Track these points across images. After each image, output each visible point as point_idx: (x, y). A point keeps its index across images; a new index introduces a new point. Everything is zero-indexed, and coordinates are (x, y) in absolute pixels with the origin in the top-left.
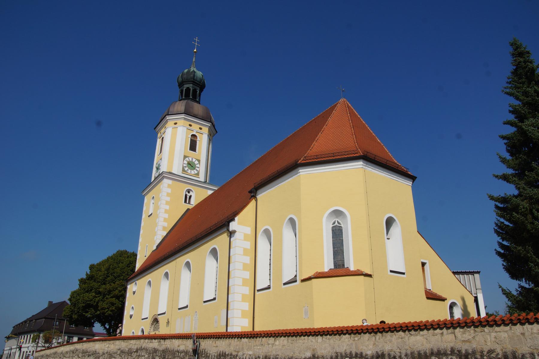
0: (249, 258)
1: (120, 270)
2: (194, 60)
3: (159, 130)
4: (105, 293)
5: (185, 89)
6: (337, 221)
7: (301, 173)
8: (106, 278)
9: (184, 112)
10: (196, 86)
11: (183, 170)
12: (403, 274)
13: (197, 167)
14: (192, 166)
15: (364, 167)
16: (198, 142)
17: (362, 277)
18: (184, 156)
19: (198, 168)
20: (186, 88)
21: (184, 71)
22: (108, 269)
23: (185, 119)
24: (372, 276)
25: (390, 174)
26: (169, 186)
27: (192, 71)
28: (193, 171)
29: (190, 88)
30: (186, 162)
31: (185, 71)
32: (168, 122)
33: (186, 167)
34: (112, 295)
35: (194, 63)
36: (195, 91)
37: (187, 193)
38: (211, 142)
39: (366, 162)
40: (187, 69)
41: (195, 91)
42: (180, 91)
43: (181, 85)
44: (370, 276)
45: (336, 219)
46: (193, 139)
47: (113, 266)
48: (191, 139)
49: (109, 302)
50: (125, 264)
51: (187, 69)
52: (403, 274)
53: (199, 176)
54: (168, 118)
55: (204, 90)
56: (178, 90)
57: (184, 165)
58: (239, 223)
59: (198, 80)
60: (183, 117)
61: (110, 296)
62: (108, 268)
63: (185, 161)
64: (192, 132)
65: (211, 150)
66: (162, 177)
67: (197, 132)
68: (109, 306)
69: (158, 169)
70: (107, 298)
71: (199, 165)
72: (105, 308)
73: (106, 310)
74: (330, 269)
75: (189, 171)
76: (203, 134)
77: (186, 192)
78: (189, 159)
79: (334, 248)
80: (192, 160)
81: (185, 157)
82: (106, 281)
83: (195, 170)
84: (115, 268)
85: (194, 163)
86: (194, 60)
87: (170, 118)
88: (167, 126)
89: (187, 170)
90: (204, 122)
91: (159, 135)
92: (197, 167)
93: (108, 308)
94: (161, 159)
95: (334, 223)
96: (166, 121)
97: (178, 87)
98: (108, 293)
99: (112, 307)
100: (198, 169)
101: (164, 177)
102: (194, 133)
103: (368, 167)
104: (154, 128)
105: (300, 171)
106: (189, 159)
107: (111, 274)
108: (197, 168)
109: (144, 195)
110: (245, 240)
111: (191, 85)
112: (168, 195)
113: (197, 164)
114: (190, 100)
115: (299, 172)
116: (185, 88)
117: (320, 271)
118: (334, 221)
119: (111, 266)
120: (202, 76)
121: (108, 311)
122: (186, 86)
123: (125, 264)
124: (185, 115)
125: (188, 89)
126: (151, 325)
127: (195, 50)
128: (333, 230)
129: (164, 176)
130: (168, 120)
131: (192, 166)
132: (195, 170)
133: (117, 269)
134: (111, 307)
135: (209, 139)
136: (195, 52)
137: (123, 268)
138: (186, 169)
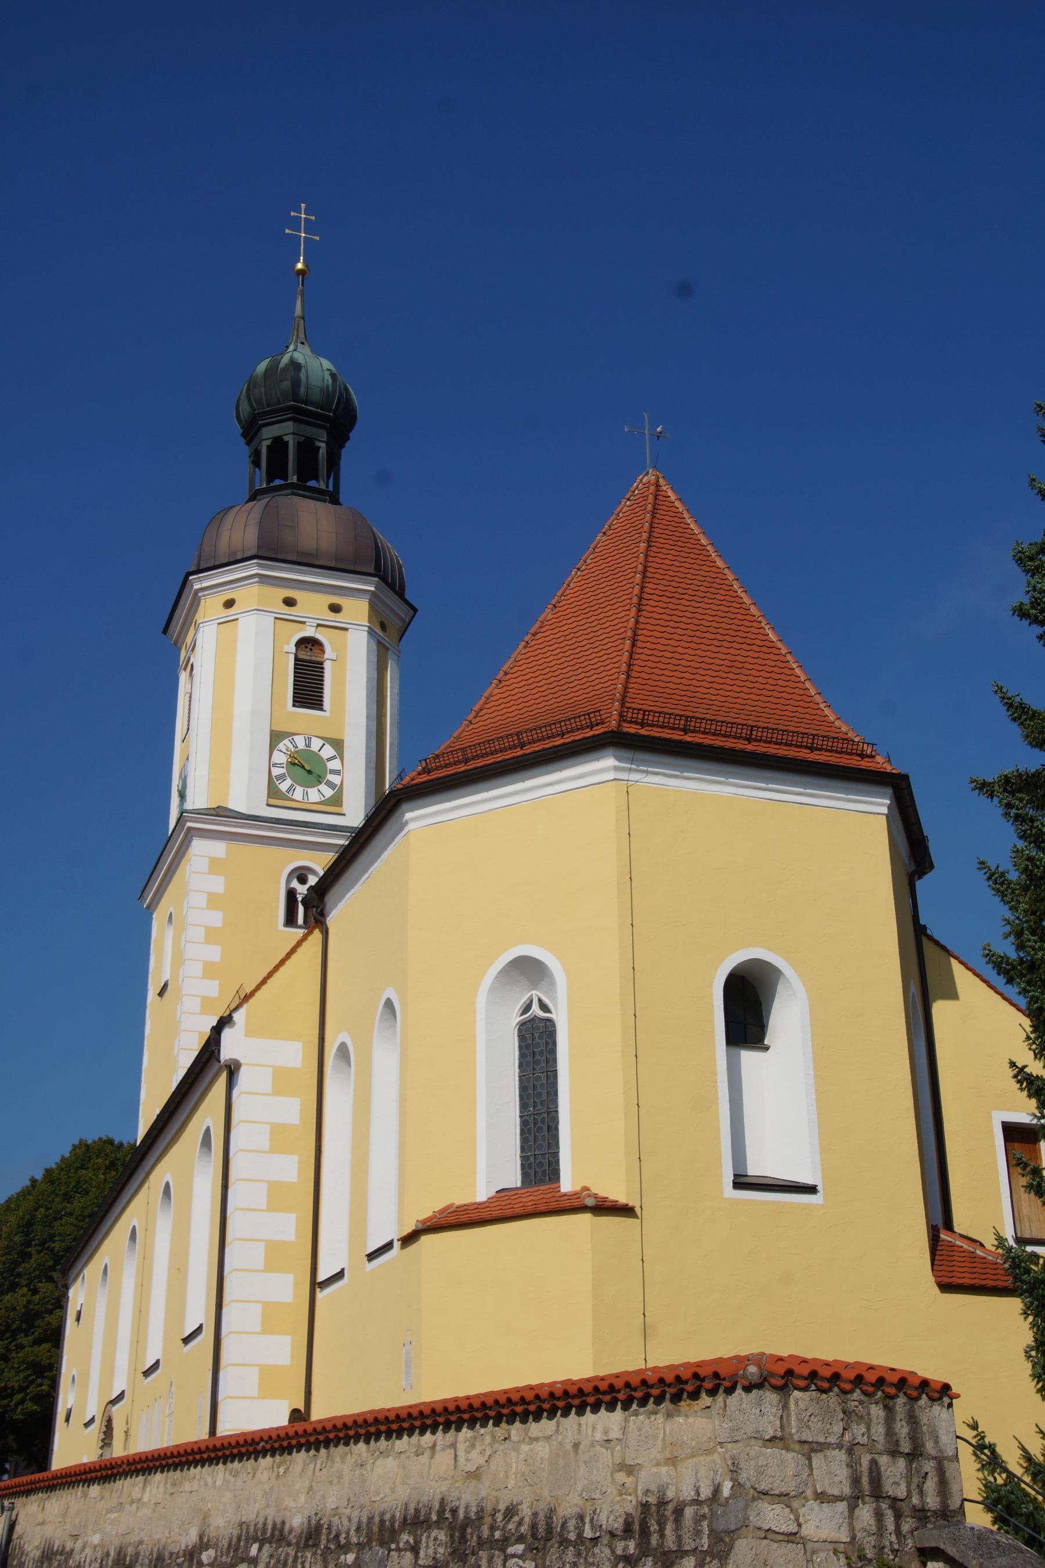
0: (295, 1159)
1: (75, 1226)
2: (298, 310)
4: (14, 1326)
6: (540, 1000)
7: (411, 826)
8: (17, 1264)
9: (254, 552)
10: (309, 428)
11: (273, 792)
12: (811, 1190)
13: (333, 772)
14: (309, 772)
15: (624, 776)
16: (328, 666)
17: (586, 1218)
18: (272, 732)
19: (337, 772)
20: (268, 442)
21: (253, 372)
22: (27, 1226)
23: (263, 579)
24: (638, 1210)
25: (763, 785)
26: (215, 866)
27: (286, 366)
28: (316, 788)
29: (286, 438)
30: (280, 758)
31: (259, 367)
32: (202, 602)
33: (282, 777)
34: (38, 1332)
35: (302, 322)
36: (307, 448)
37: (295, 884)
38: (390, 654)
39: (628, 754)
40: (268, 360)
41: (307, 448)
42: (252, 458)
43: (250, 430)
44: (626, 1211)
45: (534, 992)
46: (303, 655)
47: (47, 1209)
48: (296, 659)
49: (23, 1362)
50: (96, 1198)
51: (268, 360)
52: (811, 1190)
53: (341, 806)
54: (197, 586)
55: (351, 435)
56: (244, 451)
57: (276, 772)
58: (251, 1032)
59: (316, 396)
60: (255, 571)
61: (30, 1338)
62: (28, 1221)
63: (276, 753)
64: (301, 630)
65: (396, 691)
66: (186, 836)
67: (319, 625)
68: (26, 1378)
69: (182, 796)
70: (22, 1347)
71: (337, 761)
72: (12, 1388)
73: (18, 1397)
74: (497, 1192)
75: (298, 793)
76: (346, 629)
77: (289, 880)
78: (293, 742)
79: (523, 1106)
80: (308, 745)
81: (276, 737)
82: (19, 1275)
83: (323, 787)
84: (55, 1219)
85: (316, 757)
86: (298, 310)
87: (205, 584)
88: (199, 617)
89: (288, 791)
92: (333, 772)
93: (22, 1389)
94: (188, 759)
95: (527, 1008)
97: (243, 441)
98: (24, 1326)
99: (39, 1381)
100: (335, 779)
101: (191, 833)
102: (309, 632)
103: (647, 772)
104: (162, 630)
105: (408, 816)
106: (293, 742)
107: (43, 1243)
108: (331, 777)
109: (148, 907)
110: (276, 1092)
111: (289, 426)
112: (214, 901)
113: (329, 760)
114: (289, 491)
115: (404, 820)
116: (265, 444)
117: (460, 1200)
118: (524, 999)
119: (42, 1209)
120: (333, 376)
121: (22, 1401)
122: (269, 433)
123: (96, 1198)
124: (259, 565)
125: (278, 446)
126: (102, 1447)
127: (300, 266)
128: (522, 1037)
129: (190, 829)
130: (200, 594)
131: (309, 772)
132: (323, 787)
133: (64, 1221)
134: (33, 1382)
135: (380, 644)
136: (301, 272)
137: (86, 1213)
138: (284, 786)
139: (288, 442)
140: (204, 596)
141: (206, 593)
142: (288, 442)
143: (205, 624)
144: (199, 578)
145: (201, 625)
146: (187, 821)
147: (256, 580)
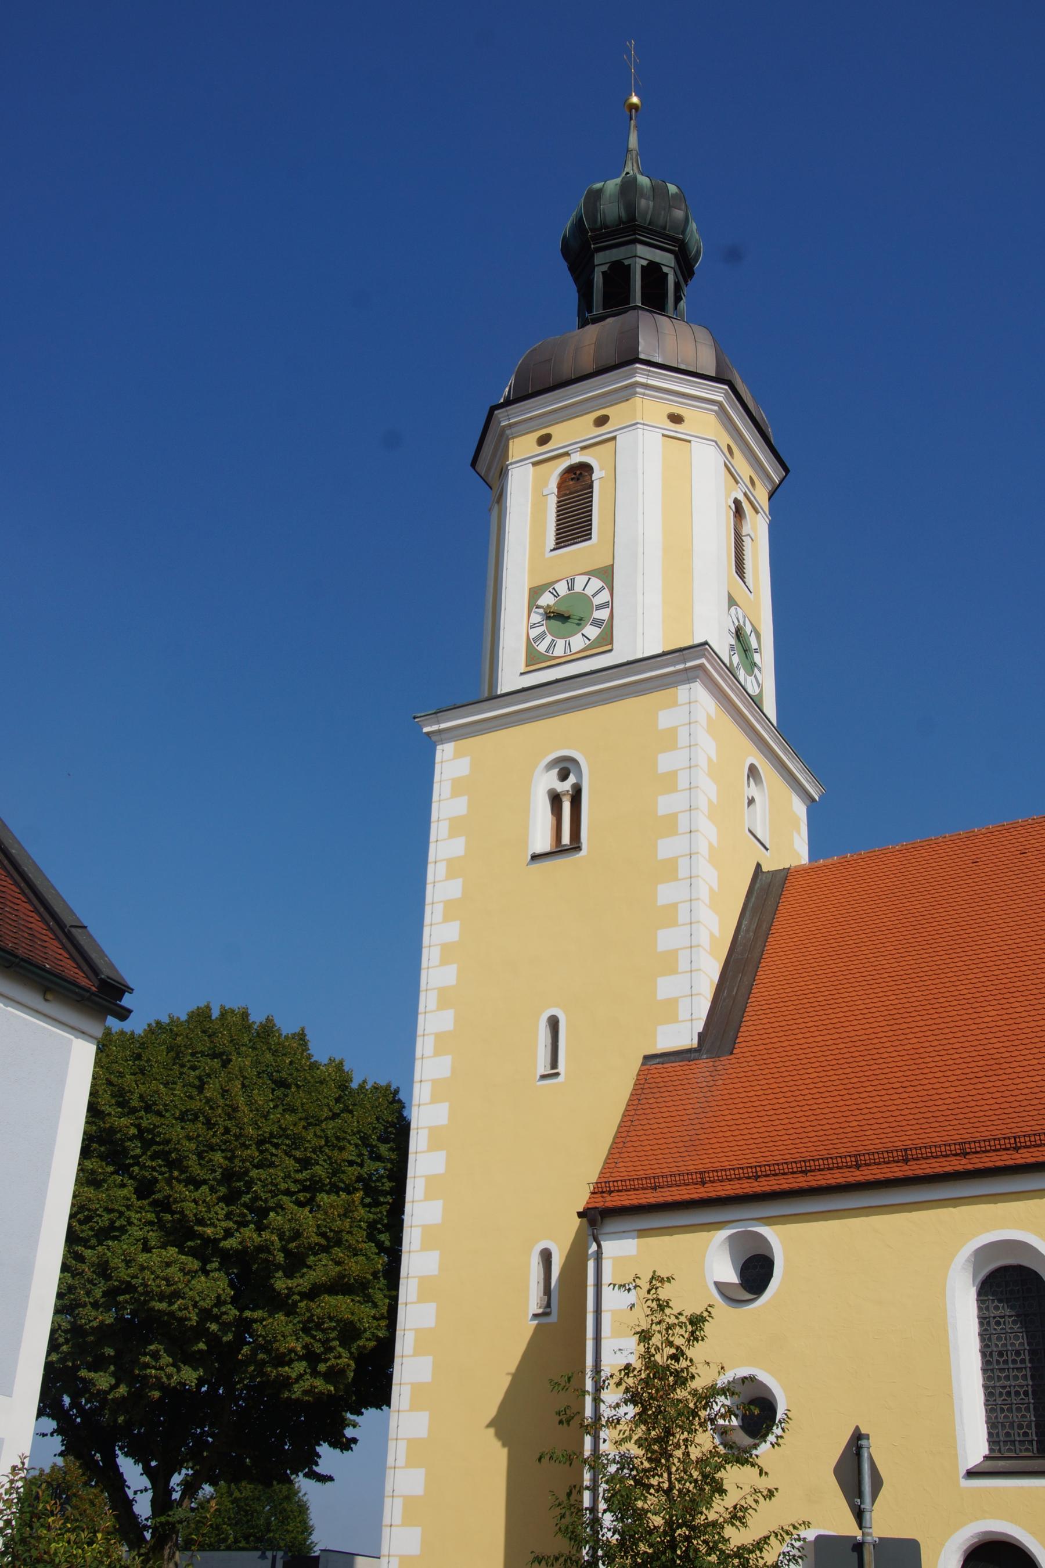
2: (633, 141)
3: (531, 419)
23: (722, 414)
29: (665, 269)
32: (637, 400)
54: (640, 379)
60: (720, 399)
86: (633, 141)
87: (650, 382)
90: (768, 461)
91: (522, 447)
96: (626, 387)
124: (726, 394)
130: (638, 390)
136: (634, 106)
139: (667, 274)
140: (644, 394)
141: (647, 392)
142: (667, 274)
143: (646, 427)
144: (649, 371)
145: (639, 426)
146: (703, 656)
147: (716, 408)
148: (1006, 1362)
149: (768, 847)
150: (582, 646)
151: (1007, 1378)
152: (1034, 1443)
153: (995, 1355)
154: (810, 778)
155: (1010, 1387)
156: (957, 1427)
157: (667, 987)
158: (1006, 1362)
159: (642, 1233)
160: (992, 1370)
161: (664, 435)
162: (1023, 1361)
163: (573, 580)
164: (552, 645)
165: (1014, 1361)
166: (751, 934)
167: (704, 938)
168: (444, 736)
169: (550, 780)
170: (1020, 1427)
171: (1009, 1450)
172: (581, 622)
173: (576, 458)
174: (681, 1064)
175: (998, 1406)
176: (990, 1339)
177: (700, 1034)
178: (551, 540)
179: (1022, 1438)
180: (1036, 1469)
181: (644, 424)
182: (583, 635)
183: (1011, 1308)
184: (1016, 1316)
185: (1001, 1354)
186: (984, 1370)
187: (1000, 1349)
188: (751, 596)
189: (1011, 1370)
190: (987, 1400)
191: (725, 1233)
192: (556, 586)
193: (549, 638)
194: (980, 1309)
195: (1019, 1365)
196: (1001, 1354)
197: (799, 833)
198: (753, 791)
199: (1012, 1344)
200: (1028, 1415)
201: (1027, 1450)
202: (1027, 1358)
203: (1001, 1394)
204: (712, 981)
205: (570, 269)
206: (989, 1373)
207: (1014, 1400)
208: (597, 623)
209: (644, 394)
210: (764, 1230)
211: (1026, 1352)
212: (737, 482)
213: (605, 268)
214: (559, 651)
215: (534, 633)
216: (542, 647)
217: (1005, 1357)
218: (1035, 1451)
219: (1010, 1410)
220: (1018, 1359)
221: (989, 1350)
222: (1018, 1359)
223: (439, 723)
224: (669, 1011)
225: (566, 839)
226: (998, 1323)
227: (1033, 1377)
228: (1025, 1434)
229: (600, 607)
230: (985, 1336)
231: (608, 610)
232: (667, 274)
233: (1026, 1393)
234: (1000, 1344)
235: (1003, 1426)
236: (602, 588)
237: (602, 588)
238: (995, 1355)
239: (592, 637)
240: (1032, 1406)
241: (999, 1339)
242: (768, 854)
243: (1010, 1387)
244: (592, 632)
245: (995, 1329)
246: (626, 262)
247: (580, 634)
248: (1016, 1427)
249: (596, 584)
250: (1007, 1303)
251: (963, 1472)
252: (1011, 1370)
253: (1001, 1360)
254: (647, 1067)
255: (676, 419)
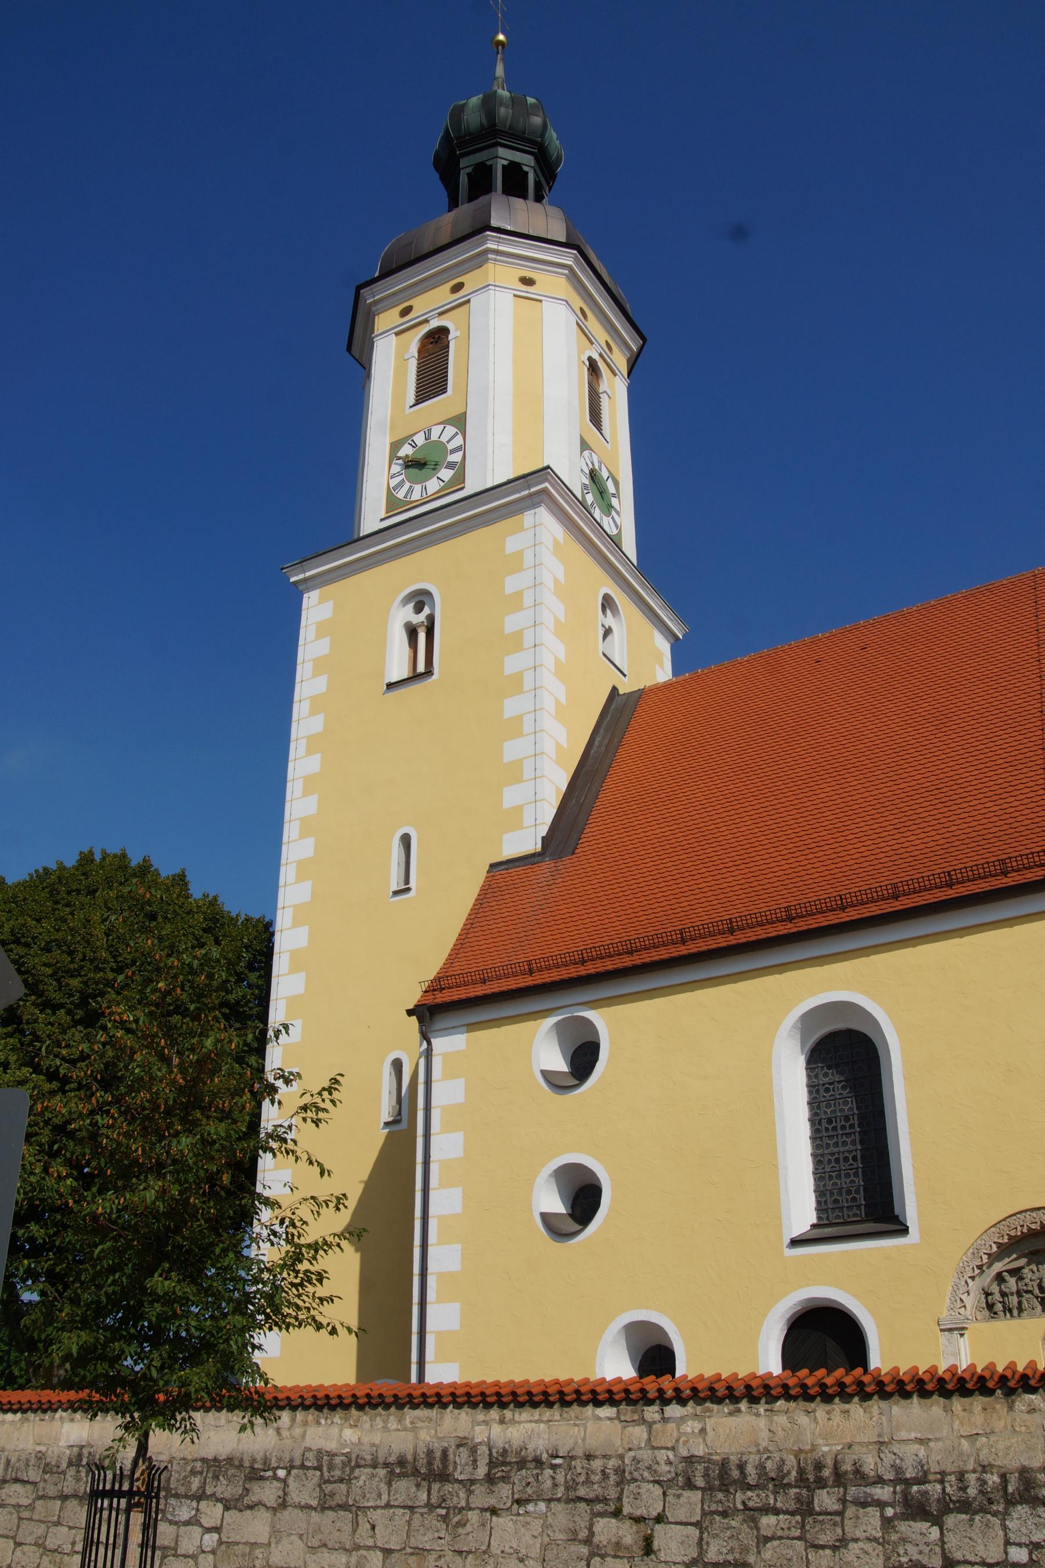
2: (500, 70)
3: (394, 294)
5: (468, 174)
23: (573, 277)
29: (525, 168)
32: (490, 266)
54: (491, 245)
60: (570, 263)
86: (500, 70)
87: (501, 248)
91: (386, 320)
124: (576, 259)
130: (490, 256)
136: (500, 43)
140: (496, 260)
141: (498, 258)
142: (527, 173)
143: (497, 288)
144: (500, 238)
145: (490, 287)
146: (546, 480)
147: (566, 272)
148: (835, 1129)
149: (626, 672)
150: (438, 488)
151: (836, 1144)
152: (863, 1207)
153: (824, 1122)
154: (660, 602)
155: (838, 1153)
156: (782, 1197)
157: (512, 796)
158: (835, 1129)
159: (471, 1027)
160: (821, 1138)
161: (515, 296)
162: (852, 1126)
163: (430, 431)
164: (410, 490)
165: (843, 1127)
166: (603, 748)
167: (548, 746)
168: (309, 584)
169: (407, 614)
170: (849, 1192)
171: (837, 1217)
172: (436, 466)
173: (435, 323)
174: (524, 868)
175: (827, 1174)
176: (819, 1107)
177: (543, 838)
178: (411, 398)
179: (850, 1204)
180: (861, 1231)
181: (495, 286)
182: (438, 478)
183: (841, 1073)
184: (845, 1081)
185: (830, 1121)
186: (813, 1139)
187: (829, 1115)
188: (609, 446)
189: (839, 1136)
190: (816, 1169)
191: (551, 1021)
192: (415, 438)
193: (407, 485)
194: (809, 1077)
195: (848, 1131)
196: (830, 1121)
197: (662, 667)
198: (610, 620)
199: (842, 1110)
200: (856, 1180)
201: (855, 1215)
202: (856, 1123)
203: (829, 1161)
204: (558, 789)
205: (440, 178)
206: (818, 1142)
207: (843, 1166)
208: (451, 466)
209: (496, 260)
210: (591, 1015)
211: (856, 1117)
212: (592, 343)
213: (469, 170)
214: (416, 496)
215: (393, 482)
216: (401, 494)
217: (834, 1124)
218: (863, 1216)
219: (839, 1177)
220: (847, 1125)
221: (819, 1118)
222: (847, 1125)
223: (304, 572)
224: (514, 818)
225: (421, 668)
226: (827, 1090)
227: (862, 1142)
228: (854, 1199)
229: (453, 451)
230: (814, 1104)
231: (461, 453)
232: (527, 173)
233: (855, 1158)
234: (828, 1111)
235: (832, 1194)
236: (457, 434)
237: (457, 434)
238: (824, 1122)
239: (446, 479)
240: (860, 1170)
241: (828, 1106)
242: (626, 680)
243: (838, 1153)
244: (446, 474)
245: (824, 1097)
246: (488, 163)
247: (435, 478)
248: (844, 1194)
249: (451, 430)
250: (836, 1068)
251: (787, 1241)
252: (839, 1136)
253: (830, 1127)
254: (492, 874)
255: (528, 282)
